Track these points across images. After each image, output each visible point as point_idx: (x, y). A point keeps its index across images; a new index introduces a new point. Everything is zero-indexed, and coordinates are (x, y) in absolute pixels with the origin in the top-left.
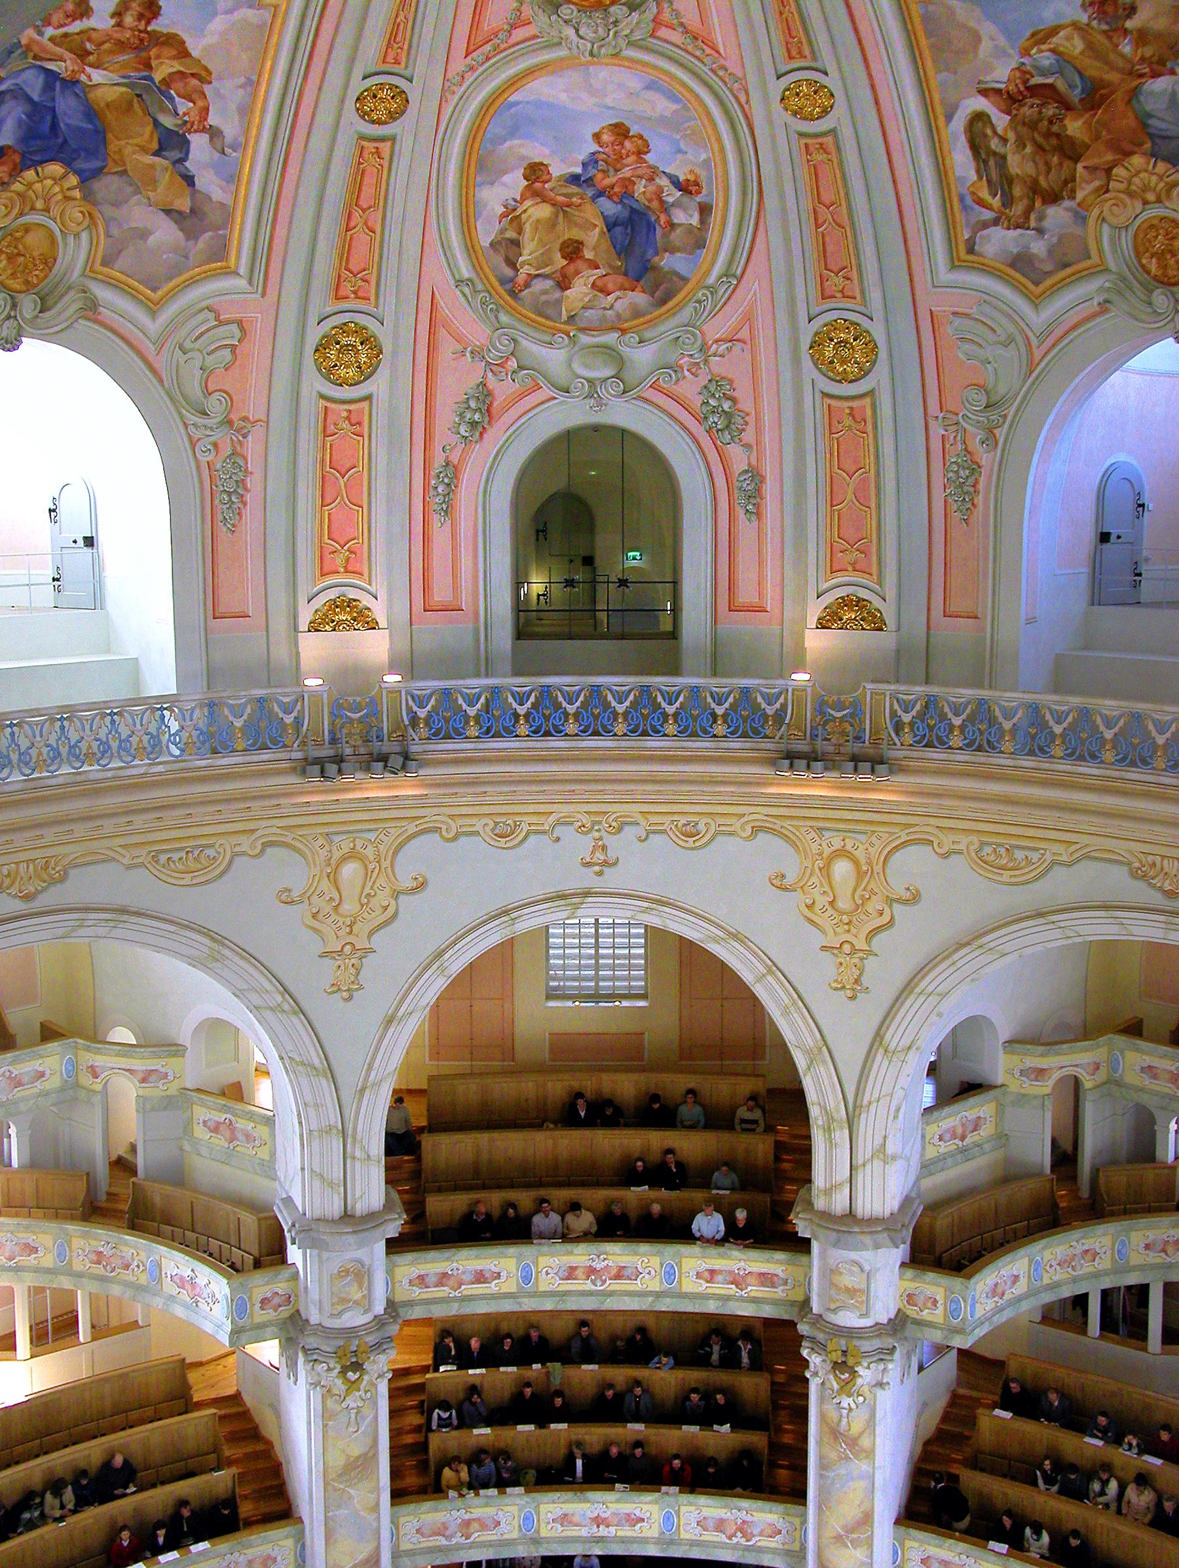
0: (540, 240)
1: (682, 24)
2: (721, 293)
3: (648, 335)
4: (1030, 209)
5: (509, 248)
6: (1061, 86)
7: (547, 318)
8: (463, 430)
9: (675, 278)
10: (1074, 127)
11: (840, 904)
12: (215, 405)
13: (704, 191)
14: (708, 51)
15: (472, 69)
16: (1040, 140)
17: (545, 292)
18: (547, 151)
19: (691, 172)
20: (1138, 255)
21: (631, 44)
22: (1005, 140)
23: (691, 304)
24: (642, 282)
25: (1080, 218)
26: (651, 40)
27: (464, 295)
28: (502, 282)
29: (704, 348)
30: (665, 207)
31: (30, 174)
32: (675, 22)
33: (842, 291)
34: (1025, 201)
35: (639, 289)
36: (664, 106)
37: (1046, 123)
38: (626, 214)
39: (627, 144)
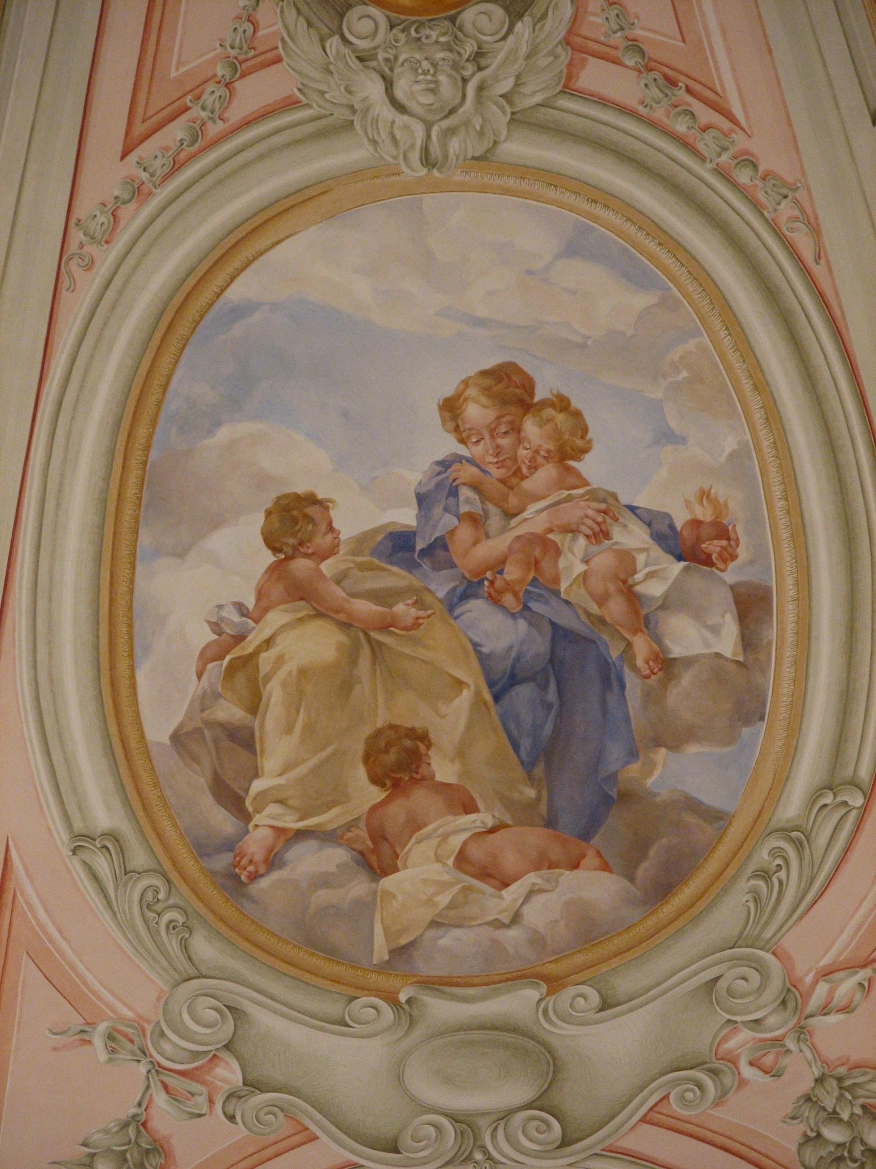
0: (309, 729)
1: (635, 46)
2: (822, 839)
3: (624, 984)
5: (227, 749)
7: (331, 953)
9: (690, 819)
13: (743, 553)
14: (705, 115)
15: (138, 192)
17: (325, 881)
19: (704, 495)
23: (744, 885)
24: (596, 841)
27: (95, 877)
28: (202, 849)
29: (792, 997)
30: (643, 616)
32: (617, 39)
35: (590, 860)
36: (609, 302)
38: (540, 645)
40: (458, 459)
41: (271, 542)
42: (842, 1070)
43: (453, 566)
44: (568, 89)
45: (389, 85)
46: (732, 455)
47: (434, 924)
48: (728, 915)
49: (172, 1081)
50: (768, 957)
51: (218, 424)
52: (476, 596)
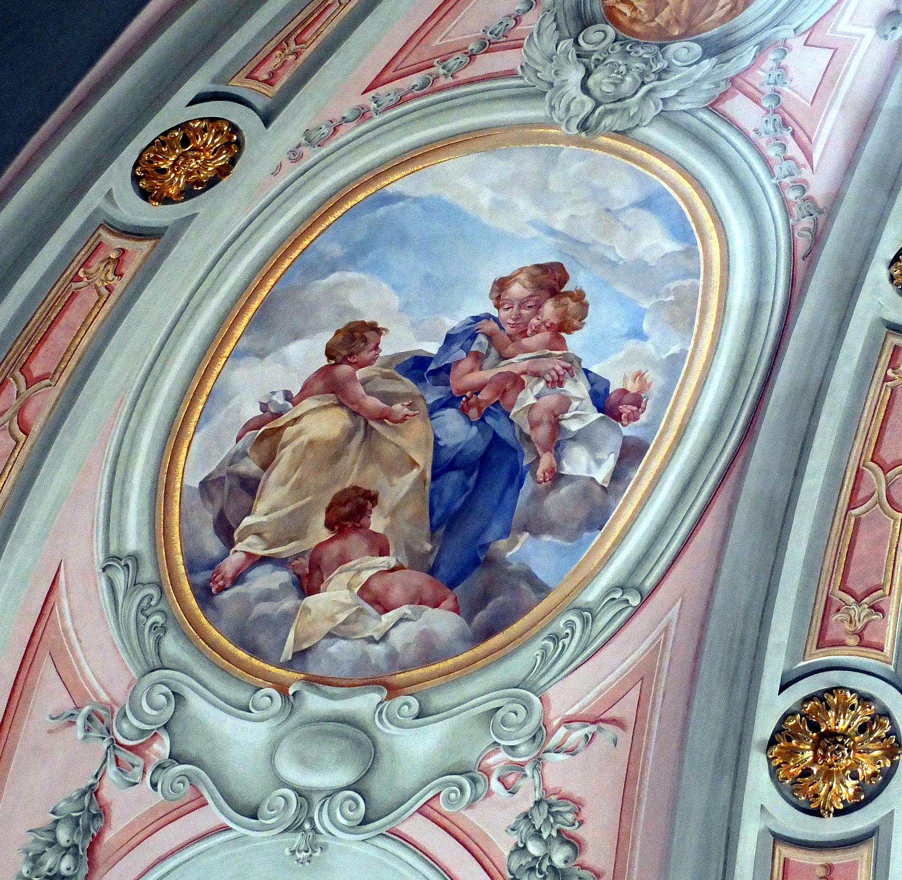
1: (776, 96)
2: (601, 623)
3: (438, 700)
7: (254, 651)
9: (524, 586)
13: (643, 418)
14: (793, 149)
17: (268, 596)
18: (395, 301)
19: (640, 375)
21: (664, 117)
23: (541, 642)
24: (458, 590)
26: (706, 117)
29: (540, 735)
30: (558, 440)
33: (860, 635)
35: (449, 603)
38: (480, 447)
39: (549, 309)
40: (488, 317)
41: (330, 353)
42: (553, 798)
43: (447, 384)
44: (712, 107)
45: (588, 73)
46: (674, 355)
47: (330, 635)
49: (124, 755)
50: (536, 700)
51: (333, 271)
52: (453, 407)
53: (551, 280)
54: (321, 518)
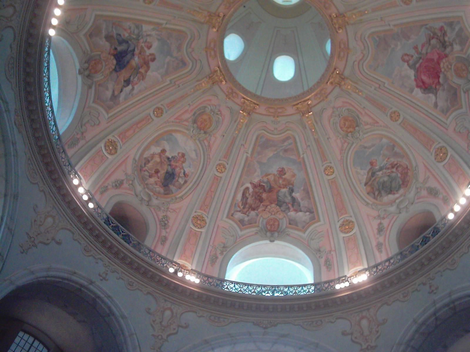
1: (209, 142)
4: (248, 211)
5: (148, 161)
6: (266, 186)
8: (114, 184)
10: (264, 196)
11: (163, 323)
12: (84, 128)
14: (209, 150)
15: (173, 122)
16: (256, 196)
20: (266, 225)
21: (199, 140)
22: (249, 194)
25: (257, 215)
28: (141, 166)
29: (168, 208)
30: (179, 177)
31: (112, 57)
34: (248, 209)
36: (193, 155)
37: (259, 193)
39: (182, 159)
40: (176, 156)
41: (161, 151)
48: (169, 200)
53: (183, 155)
54: (154, 170)
